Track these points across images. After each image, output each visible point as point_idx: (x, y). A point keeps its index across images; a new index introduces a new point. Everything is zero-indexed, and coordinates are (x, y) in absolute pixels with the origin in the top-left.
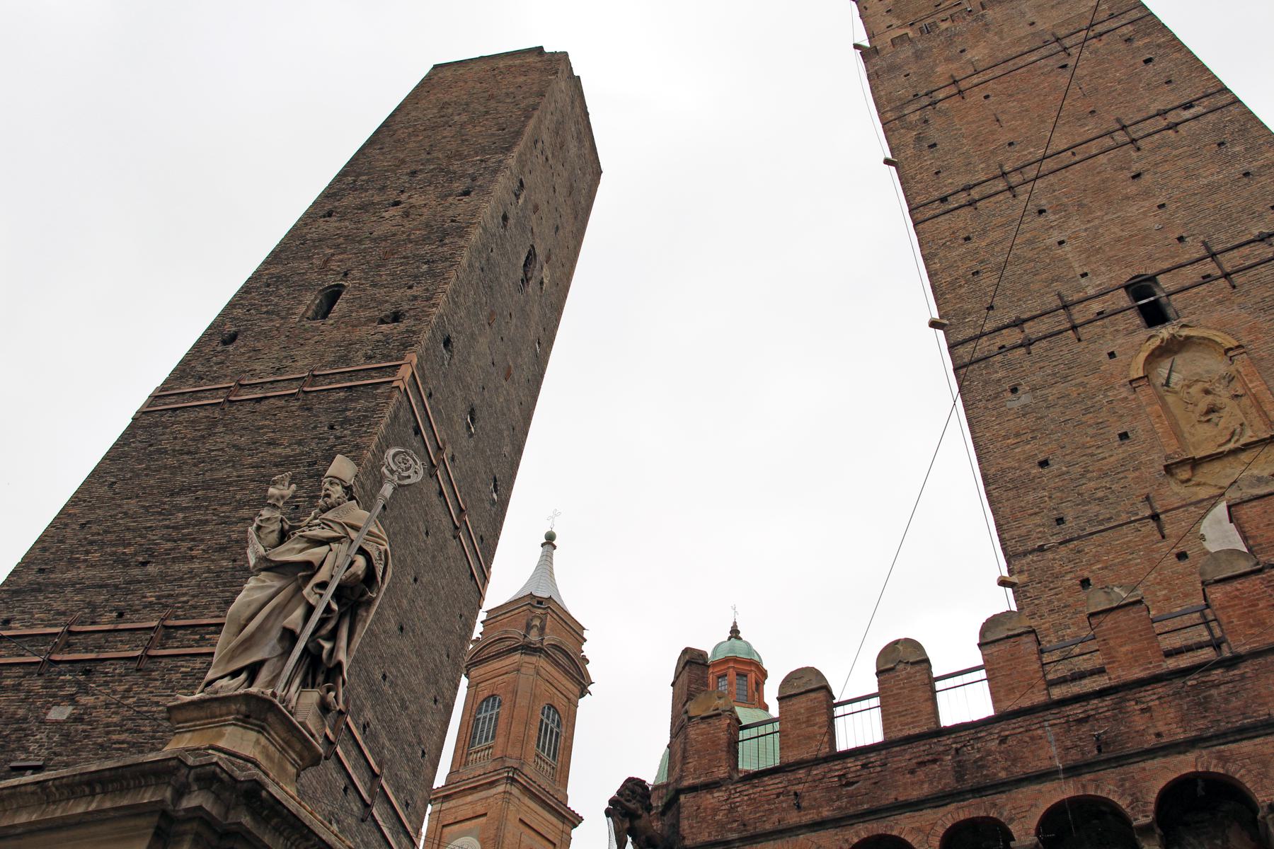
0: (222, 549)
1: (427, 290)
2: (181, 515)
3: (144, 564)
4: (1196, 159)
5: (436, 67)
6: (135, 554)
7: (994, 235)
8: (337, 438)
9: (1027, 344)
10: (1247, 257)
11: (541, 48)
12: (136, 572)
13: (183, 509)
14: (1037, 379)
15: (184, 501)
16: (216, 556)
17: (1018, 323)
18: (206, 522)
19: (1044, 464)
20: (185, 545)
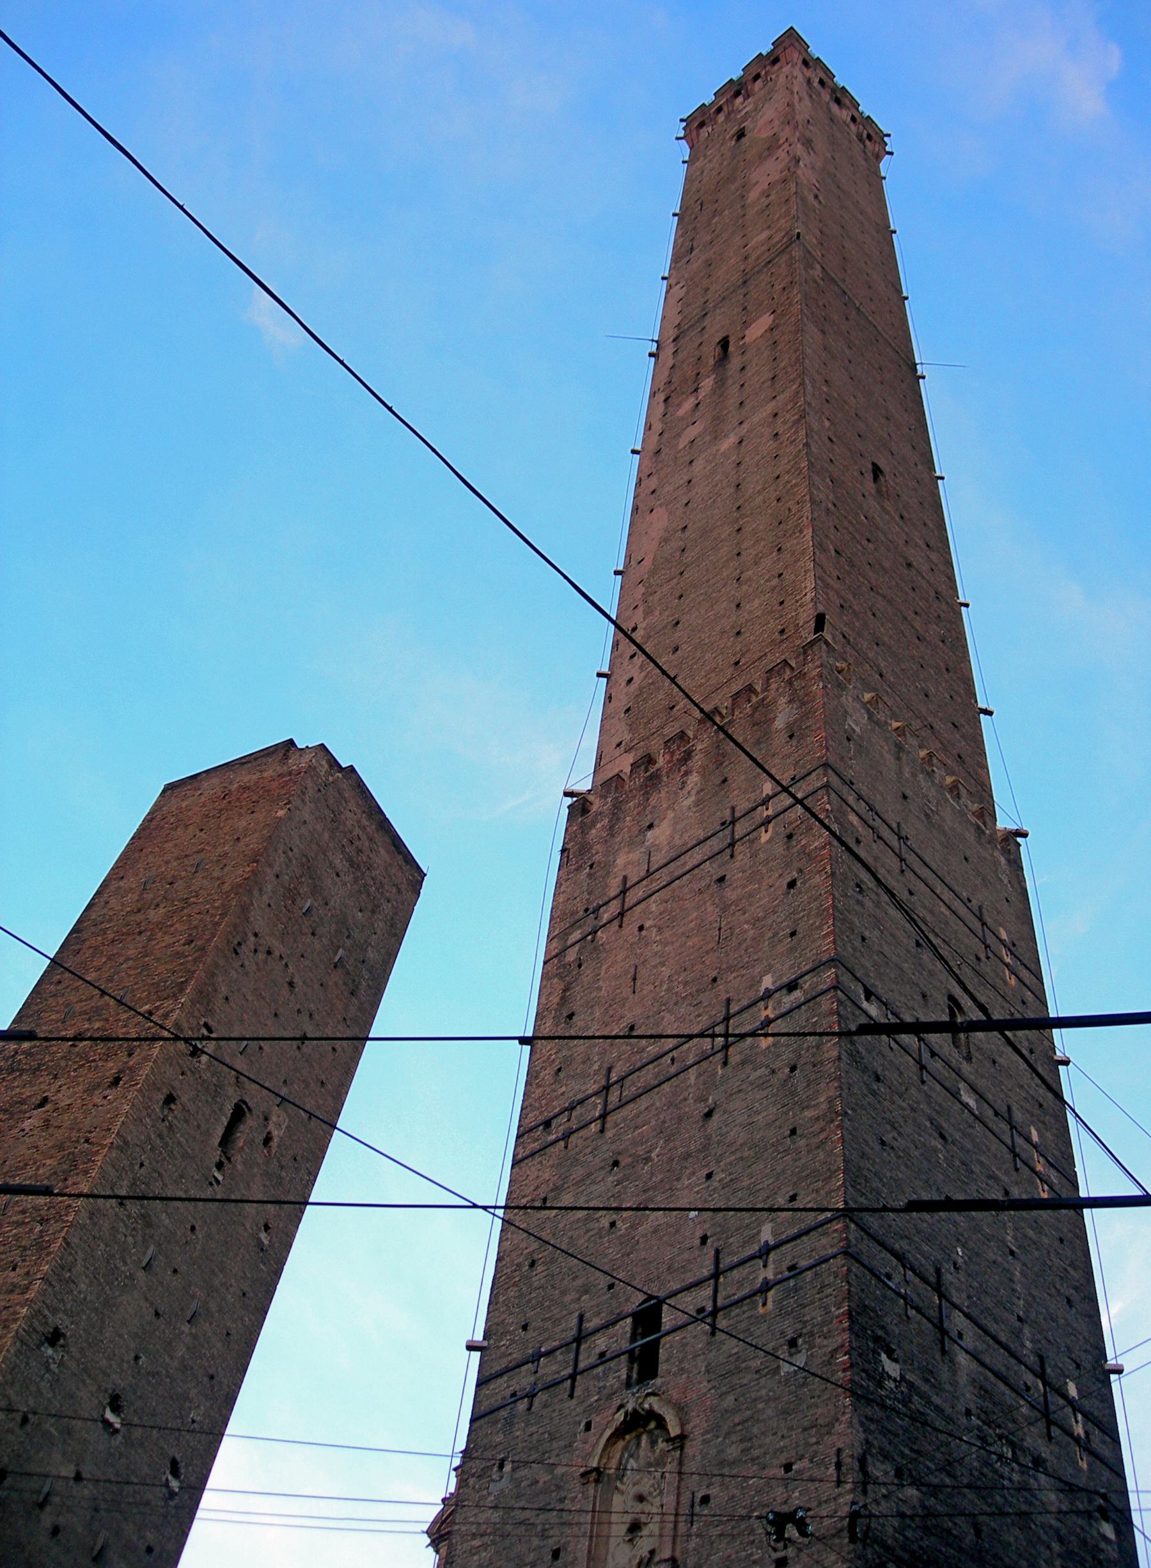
1: (28, 1273)
4: (765, 1093)
5: (170, 788)
10: (740, 1283)
11: (291, 742)
17: (536, 1357)
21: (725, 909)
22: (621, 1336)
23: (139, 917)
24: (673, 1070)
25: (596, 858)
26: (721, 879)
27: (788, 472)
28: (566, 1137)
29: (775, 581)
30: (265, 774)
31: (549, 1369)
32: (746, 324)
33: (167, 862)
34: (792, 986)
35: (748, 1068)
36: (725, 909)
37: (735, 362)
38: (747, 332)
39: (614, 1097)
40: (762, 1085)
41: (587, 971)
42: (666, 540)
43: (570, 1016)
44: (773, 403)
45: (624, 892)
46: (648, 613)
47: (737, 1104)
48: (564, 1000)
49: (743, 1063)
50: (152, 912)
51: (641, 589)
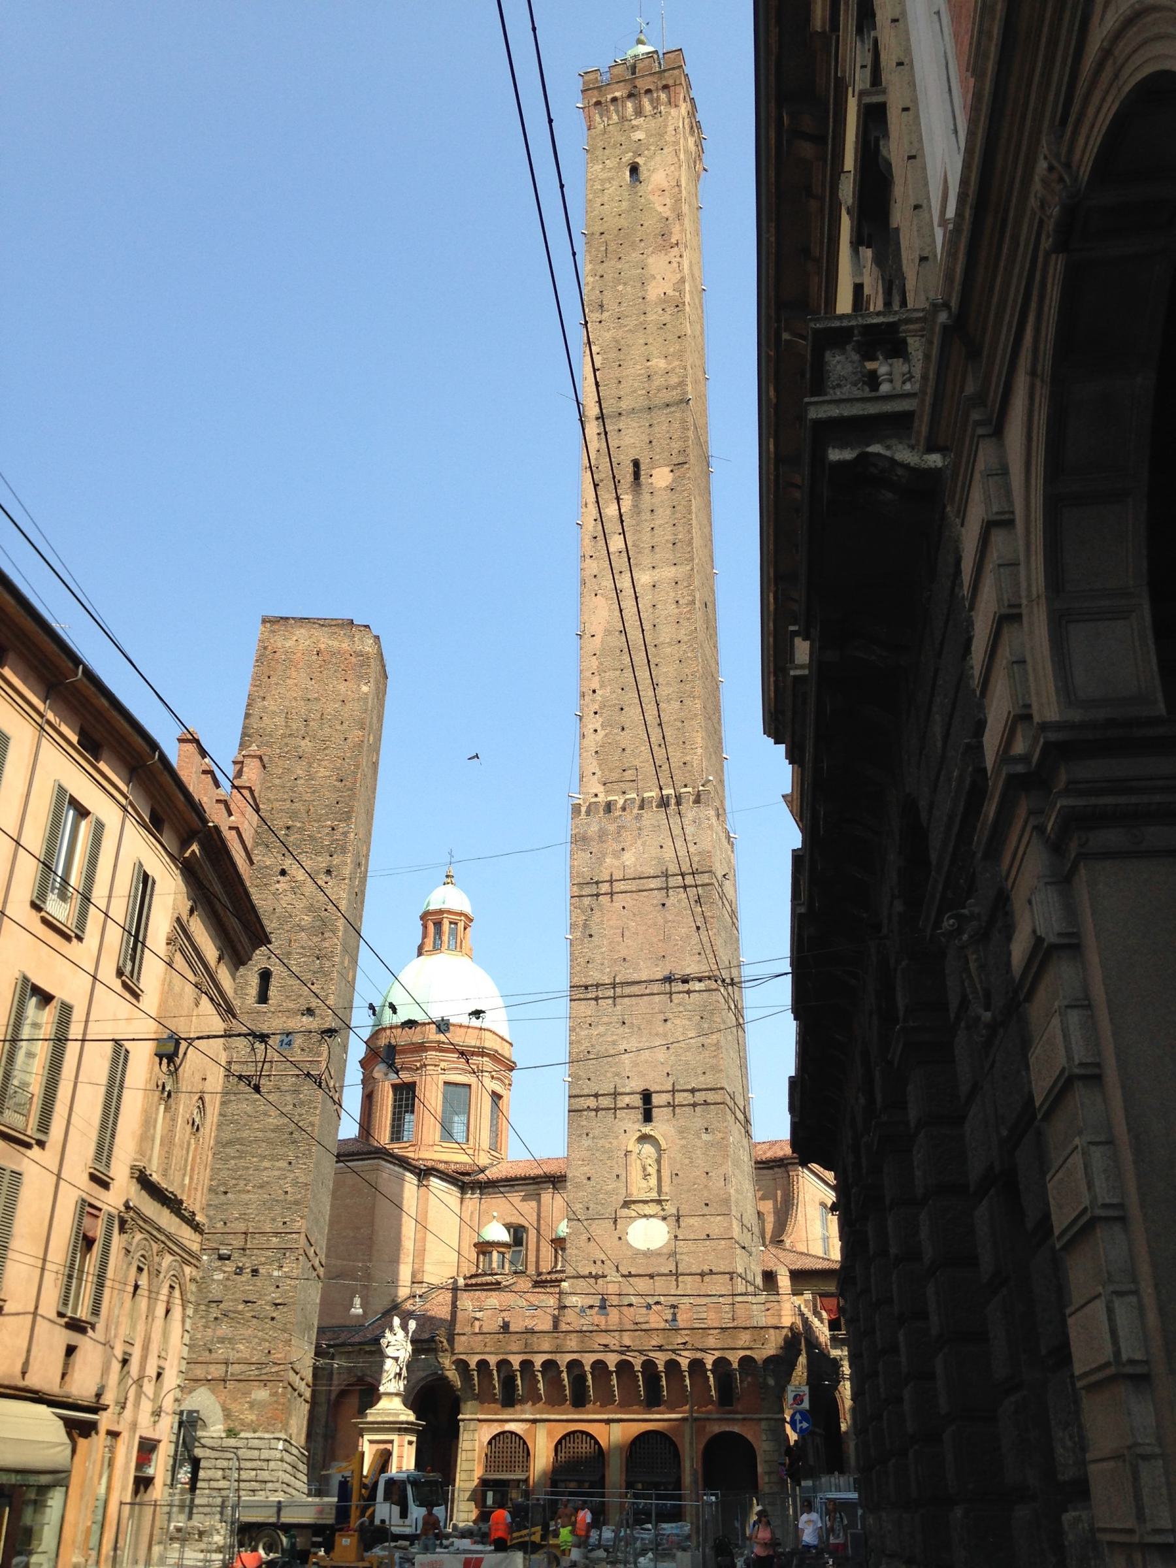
0: (261, 1187)
2: (233, 1162)
3: (226, 1193)
6: (218, 1186)
7: (602, 1029)
8: (300, 1115)
9: (597, 1110)
12: (223, 1197)
13: (233, 1158)
14: (597, 1132)
15: (231, 1151)
16: (260, 1191)
17: (596, 1096)
18: (248, 1168)
19: (589, 1179)
20: (242, 1183)
21: (666, 922)
22: (637, 1101)
23: (292, 741)
24: (648, 991)
25: (594, 850)
26: (664, 905)
27: (686, 643)
28: (596, 999)
29: (679, 724)
30: (344, 645)
31: (605, 1102)
32: (653, 464)
33: (295, 698)
34: (700, 980)
35: (681, 1009)
36: (666, 922)
37: (646, 497)
38: (654, 472)
39: (618, 990)
40: (690, 1019)
41: (597, 913)
42: (608, 632)
43: (591, 936)
44: (673, 569)
45: (611, 881)
46: (601, 687)
47: (677, 1021)
48: (585, 926)
49: (679, 1004)
50: (303, 743)
51: (594, 662)
